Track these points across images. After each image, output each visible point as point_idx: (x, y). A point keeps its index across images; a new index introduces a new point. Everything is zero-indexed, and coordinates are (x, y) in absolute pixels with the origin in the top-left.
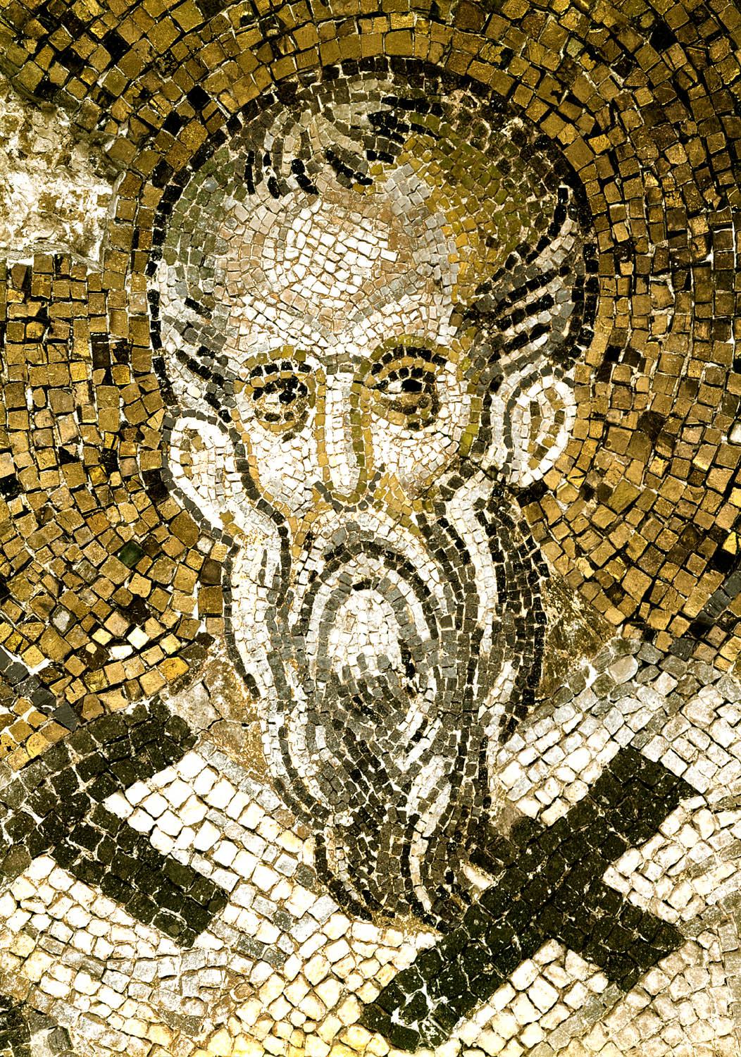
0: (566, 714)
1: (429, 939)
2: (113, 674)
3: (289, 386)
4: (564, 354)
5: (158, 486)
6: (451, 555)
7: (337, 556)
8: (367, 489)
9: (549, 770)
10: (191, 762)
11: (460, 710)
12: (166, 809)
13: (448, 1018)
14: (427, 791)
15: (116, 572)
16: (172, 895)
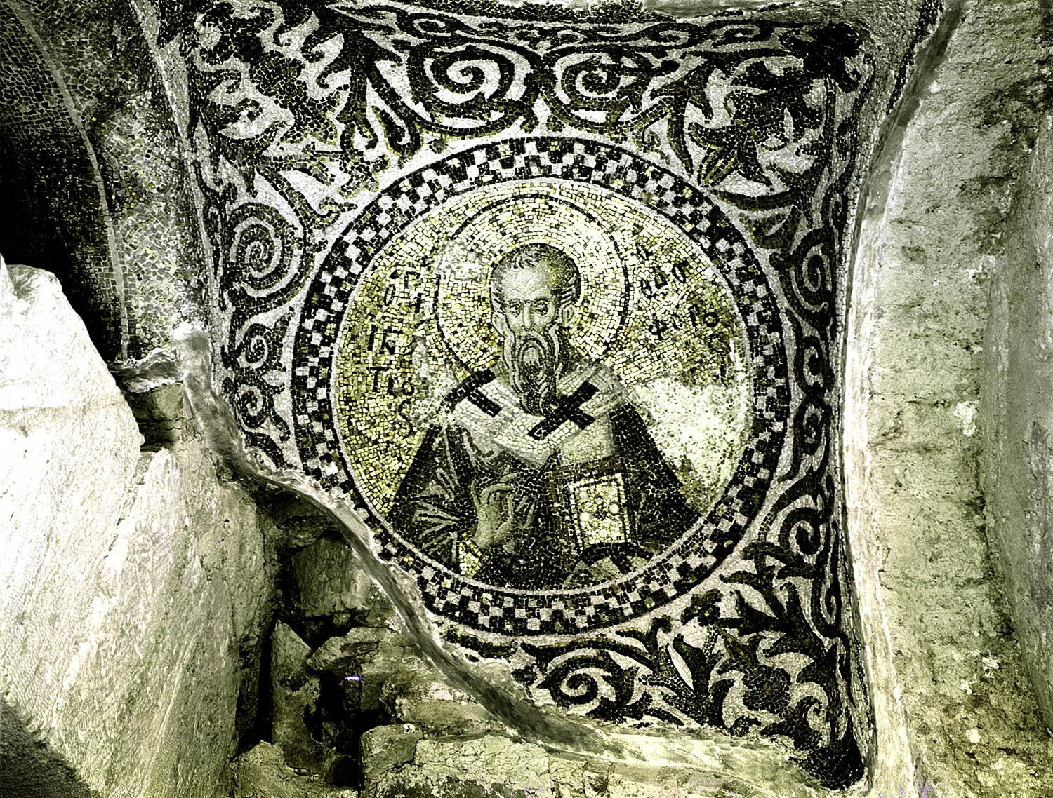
0: (573, 374)
1: (543, 418)
2: (480, 363)
3: (518, 306)
4: (574, 300)
5: (490, 326)
6: (550, 341)
7: (526, 341)
8: (533, 325)
9: (569, 385)
10: (495, 381)
11: (550, 373)
12: (490, 390)
13: (545, 434)
14: (543, 390)
15: (481, 342)
16: (490, 407)
